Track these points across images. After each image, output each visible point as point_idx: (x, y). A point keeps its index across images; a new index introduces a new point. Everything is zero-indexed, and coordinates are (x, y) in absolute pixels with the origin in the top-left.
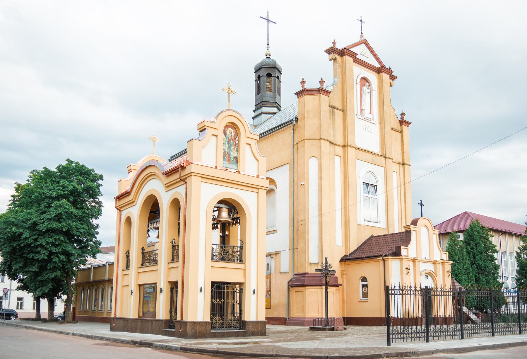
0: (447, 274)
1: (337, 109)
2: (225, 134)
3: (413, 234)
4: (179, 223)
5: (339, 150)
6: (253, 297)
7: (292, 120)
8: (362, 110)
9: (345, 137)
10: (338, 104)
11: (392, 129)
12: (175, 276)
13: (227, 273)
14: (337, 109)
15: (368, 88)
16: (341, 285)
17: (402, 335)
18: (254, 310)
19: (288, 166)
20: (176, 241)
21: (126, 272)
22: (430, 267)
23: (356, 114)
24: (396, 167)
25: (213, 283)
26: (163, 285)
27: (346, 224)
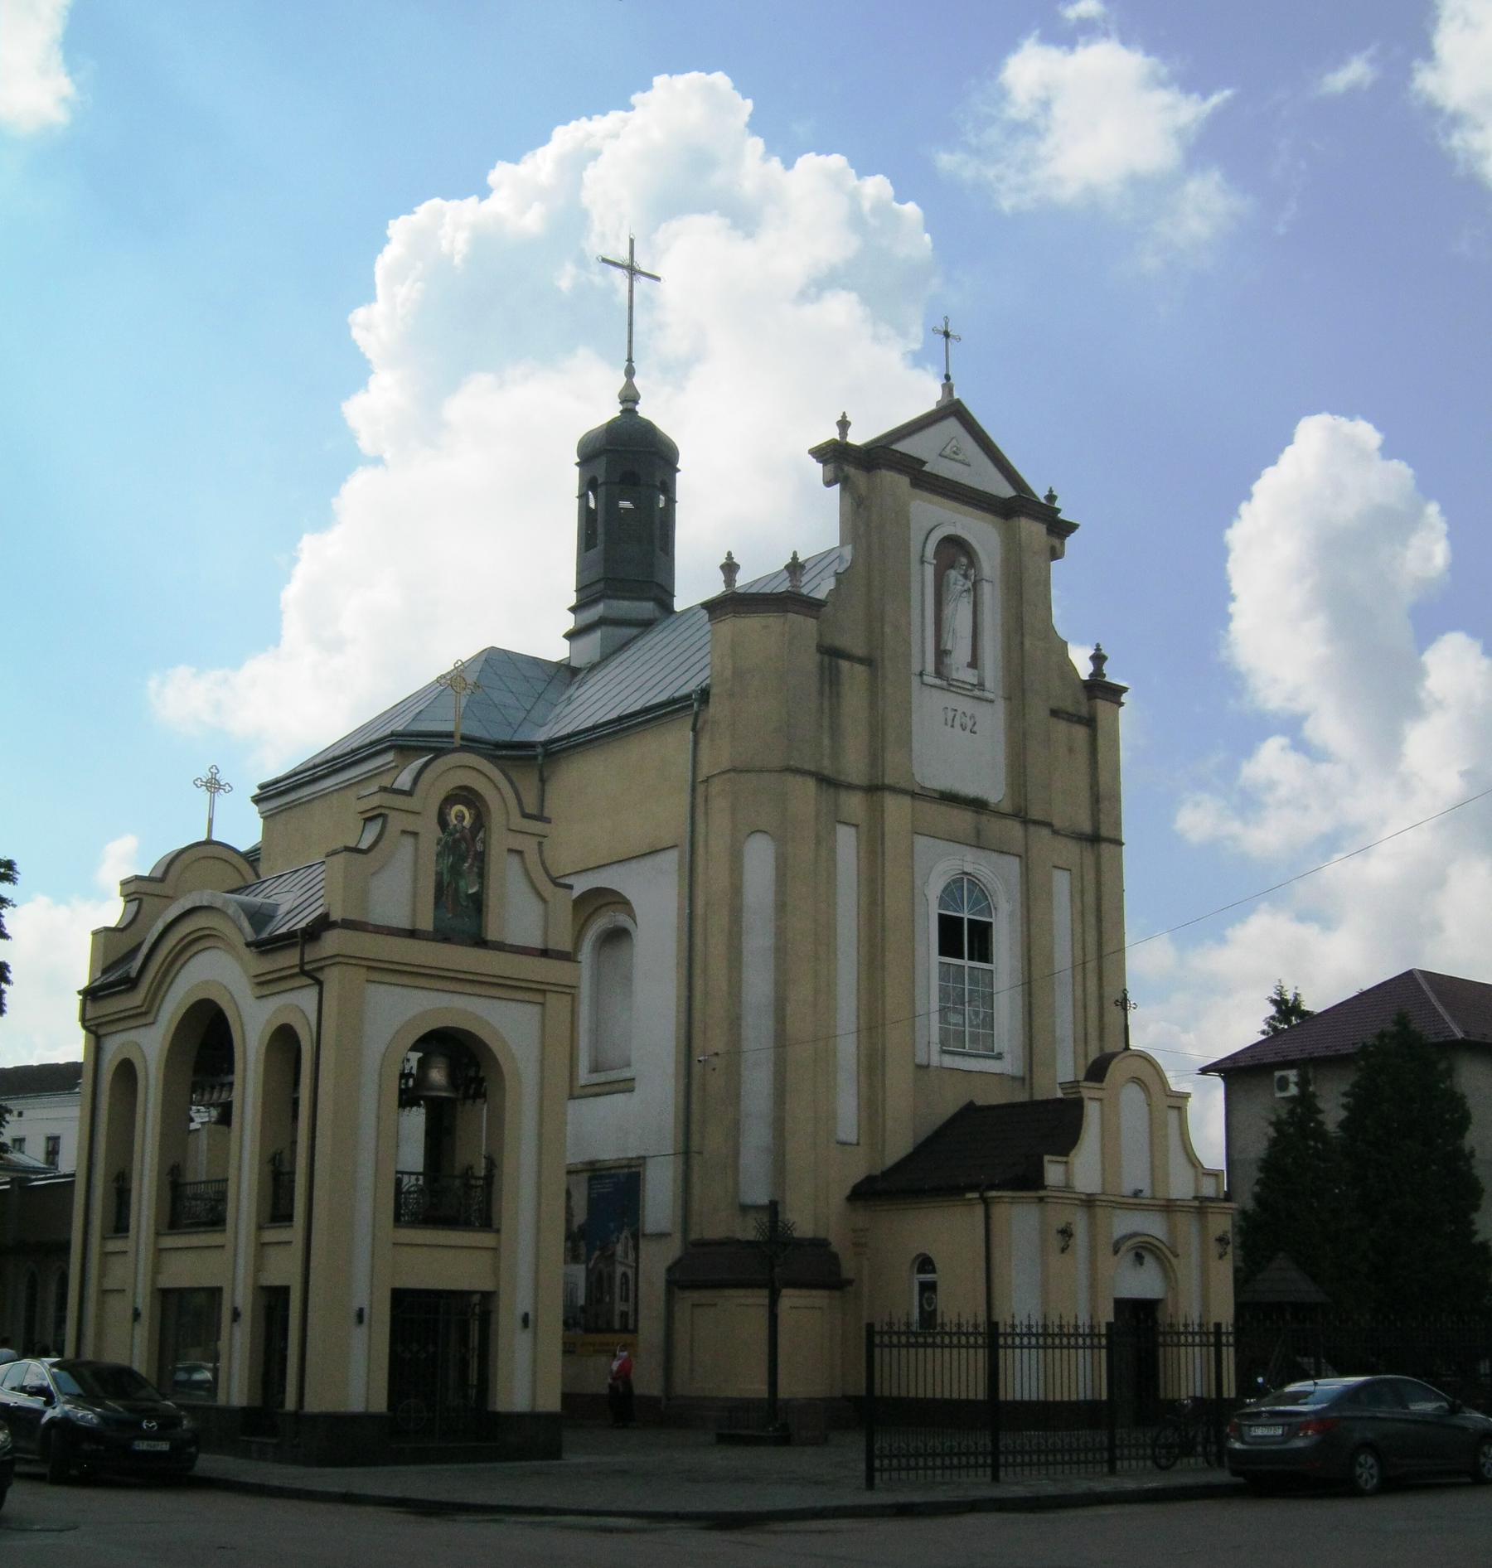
0: (1214, 1249)
1: (849, 657)
2: (443, 822)
3: (1092, 1111)
4: (295, 1103)
5: (854, 804)
6: (523, 1339)
7: (688, 697)
8: (941, 654)
9: (875, 757)
10: (853, 642)
11: (1055, 713)
12: (283, 1270)
13: (444, 1262)
14: (849, 657)
15: (966, 576)
16: (850, 1282)
17: (886, 1462)
18: (527, 1373)
19: (673, 855)
20: (286, 1155)
21: (113, 1245)
22: (1153, 1226)
23: (916, 668)
24: (1070, 851)
25: (400, 1297)
26: (241, 1295)
27: (873, 1064)
